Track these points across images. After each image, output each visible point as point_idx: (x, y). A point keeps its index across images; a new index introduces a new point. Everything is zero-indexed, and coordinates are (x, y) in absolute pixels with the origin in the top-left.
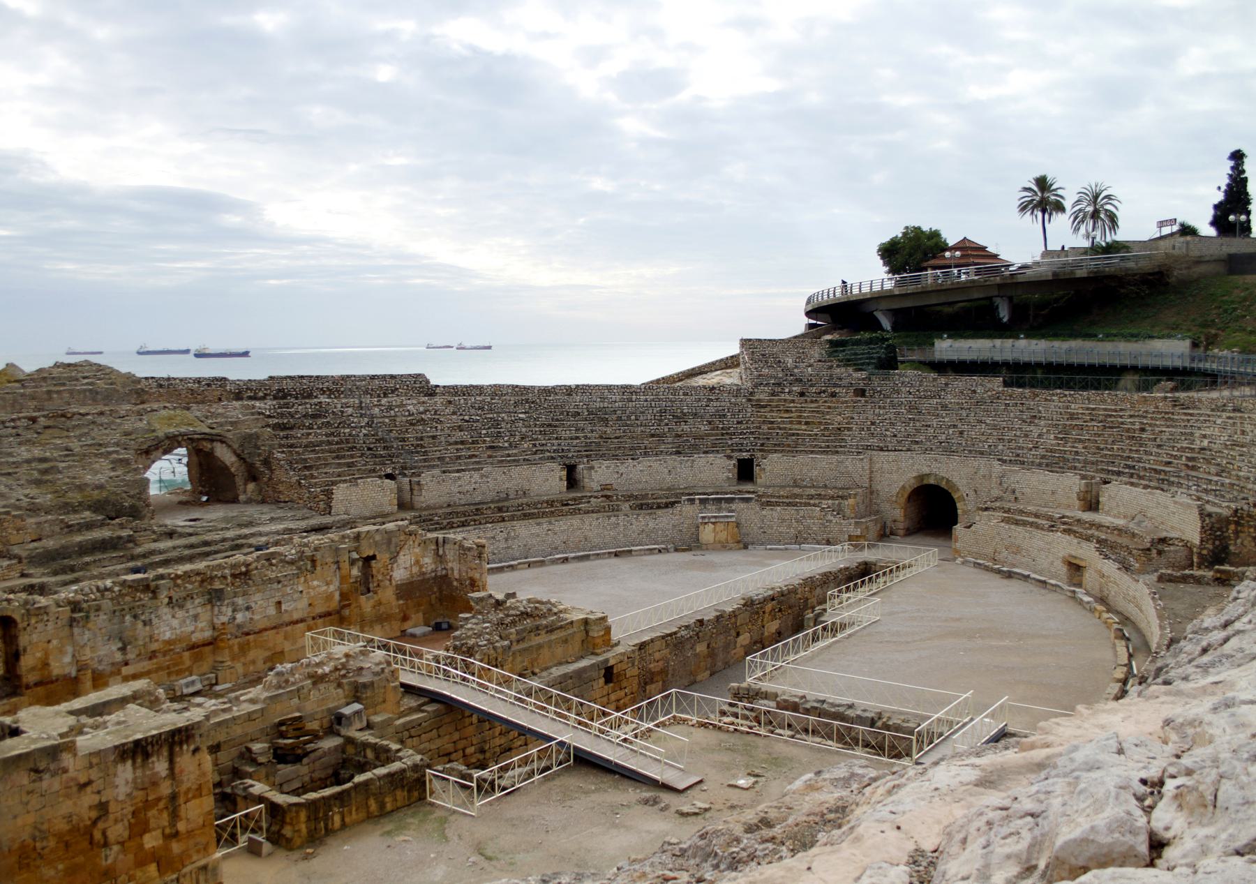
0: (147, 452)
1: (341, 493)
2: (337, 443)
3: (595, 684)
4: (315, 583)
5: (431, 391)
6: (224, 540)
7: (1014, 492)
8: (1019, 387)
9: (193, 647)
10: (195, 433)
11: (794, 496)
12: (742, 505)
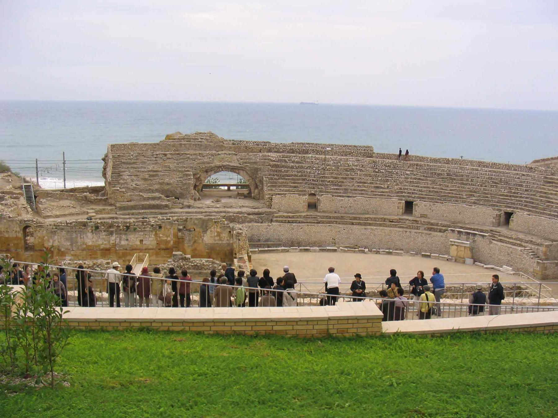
0: (207, 172)
1: (276, 199)
2: (300, 176)
6: (206, 212)
9: (102, 250)
10: (229, 165)
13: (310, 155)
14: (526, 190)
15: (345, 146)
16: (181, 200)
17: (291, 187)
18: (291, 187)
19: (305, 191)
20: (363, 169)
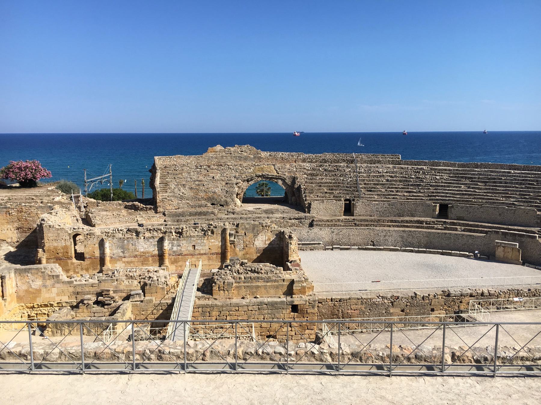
2: (334, 183)
3: (284, 312)
4: (213, 240)
12: (529, 239)
13: (342, 165)
16: (225, 208)
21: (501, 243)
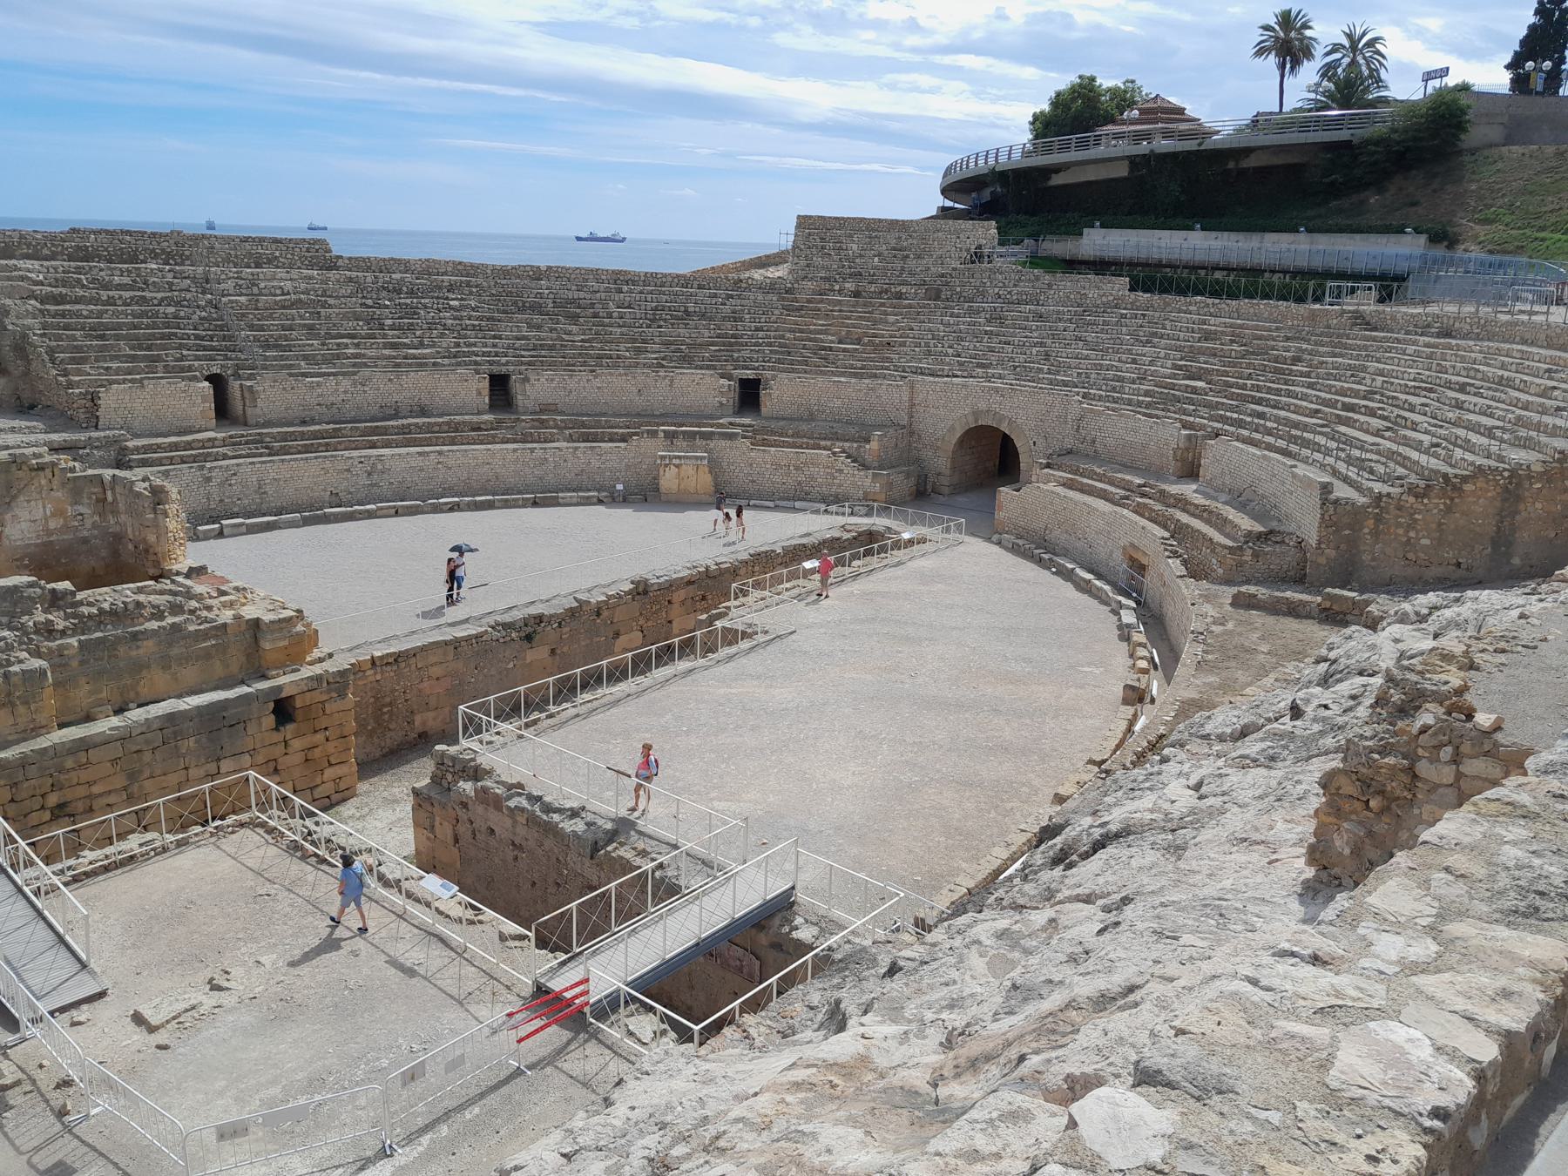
5: (331, 264)
7: (1094, 442)
8: (1145, 291)
11: (808, 428)
12: (723, 443)
14: (757, 329)
15: (245, 240)
17: (133, 358)
18: (133, 358)
19: (190, 368)
20: (331, 301)
21: (671, 458)
